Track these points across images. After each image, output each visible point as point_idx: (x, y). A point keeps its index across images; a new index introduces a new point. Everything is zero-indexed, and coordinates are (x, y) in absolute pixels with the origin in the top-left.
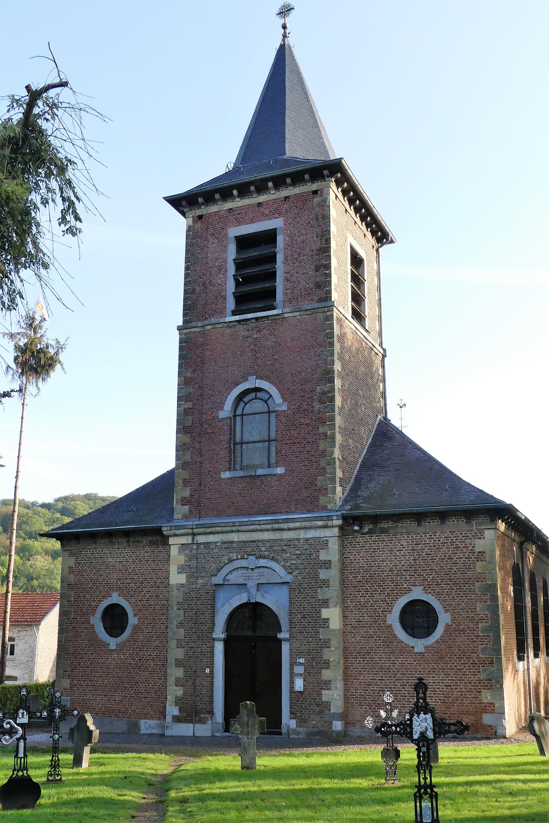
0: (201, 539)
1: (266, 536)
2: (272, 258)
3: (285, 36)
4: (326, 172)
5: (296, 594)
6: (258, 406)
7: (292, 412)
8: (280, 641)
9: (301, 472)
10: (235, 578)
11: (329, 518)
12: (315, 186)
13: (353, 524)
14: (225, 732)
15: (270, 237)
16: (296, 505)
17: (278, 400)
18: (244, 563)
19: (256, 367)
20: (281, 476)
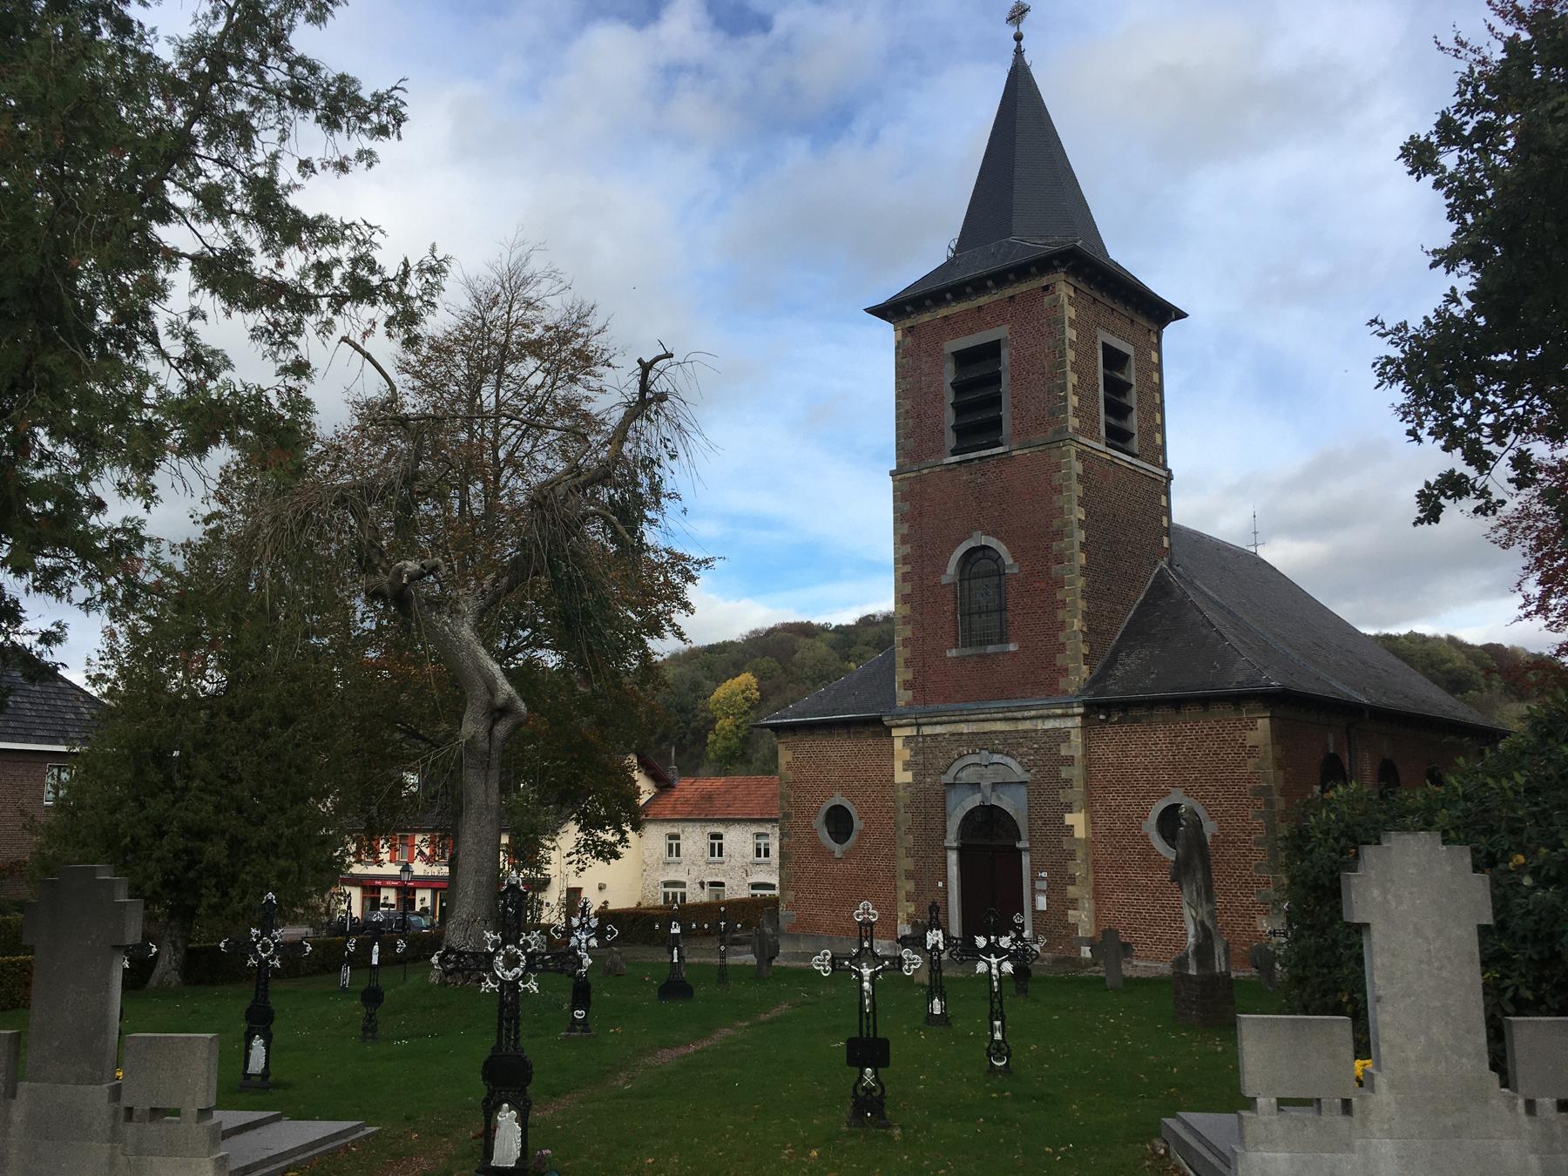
0: (927, 730)
1: (999, 726)
2: (996, 379)
3: (1019, 52)
4: (1056, 263)
8: (1019, 851)
10: (966, 776)
11: (1069, 705)
12: (1044, 281)
13: (1098, 713)
15: (993, 349)
18: (975, 759)
20: (1015, 654)
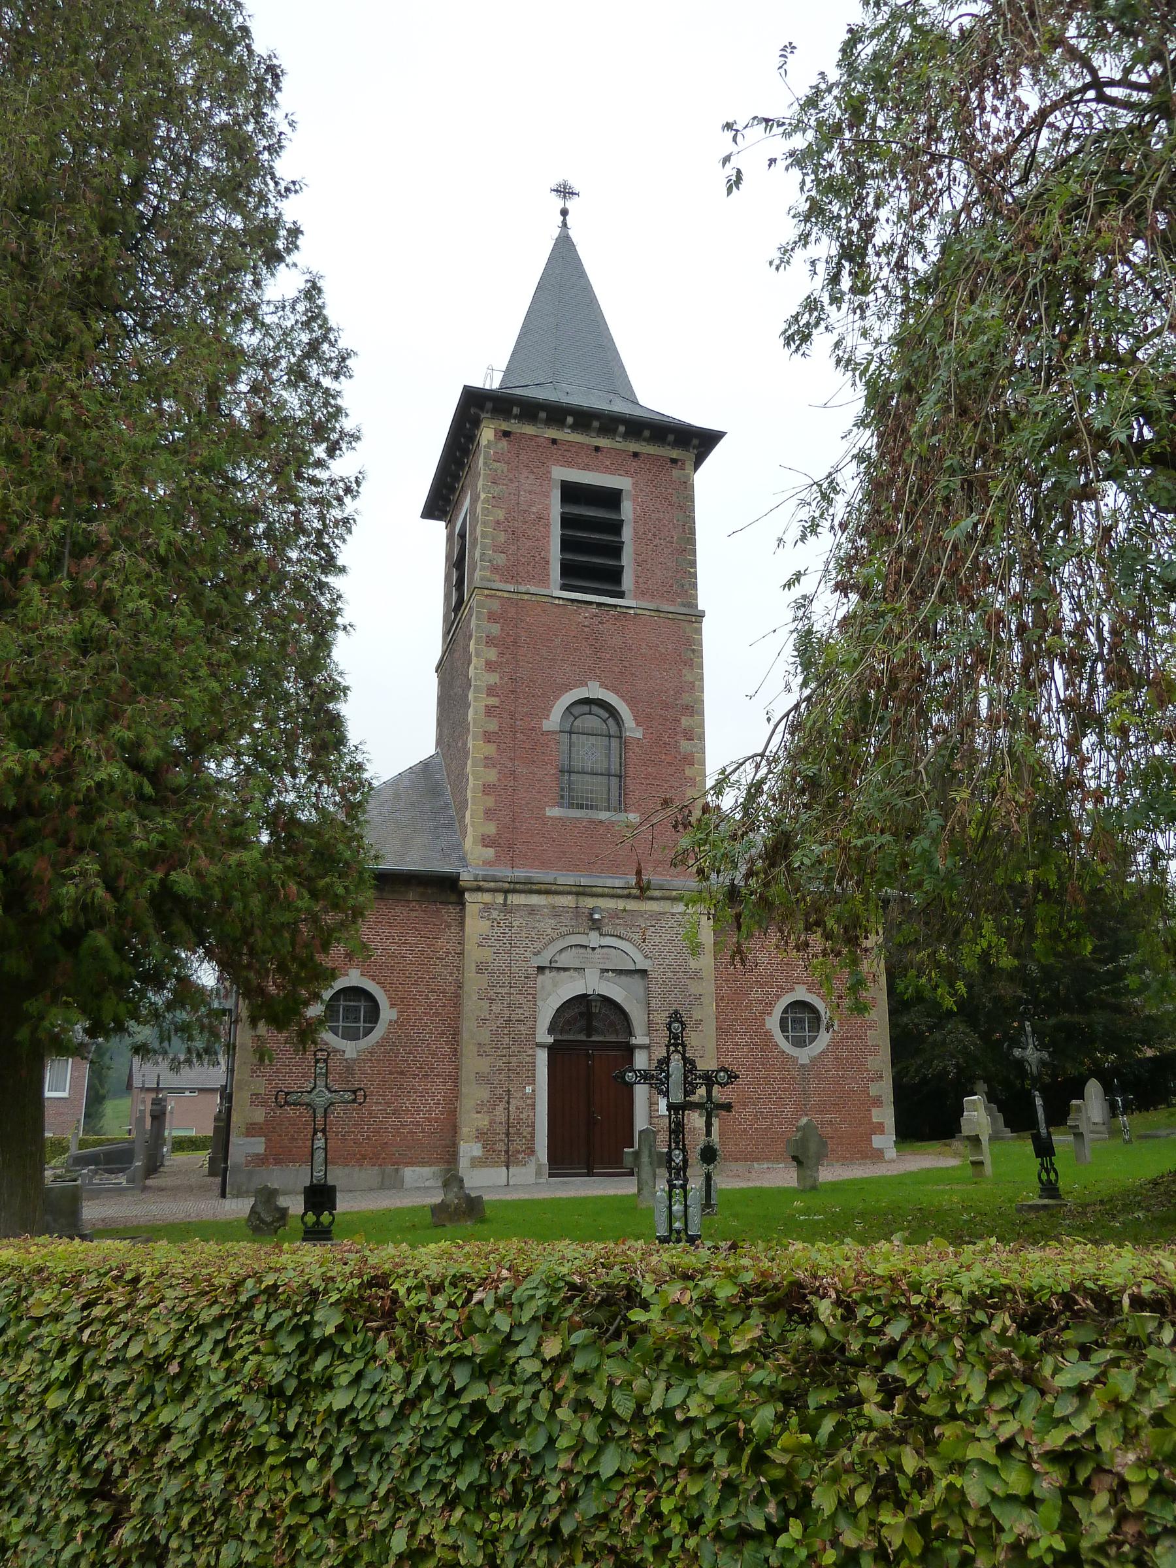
3: (564, 224)
12: (674, 454)
15: (611, 498)
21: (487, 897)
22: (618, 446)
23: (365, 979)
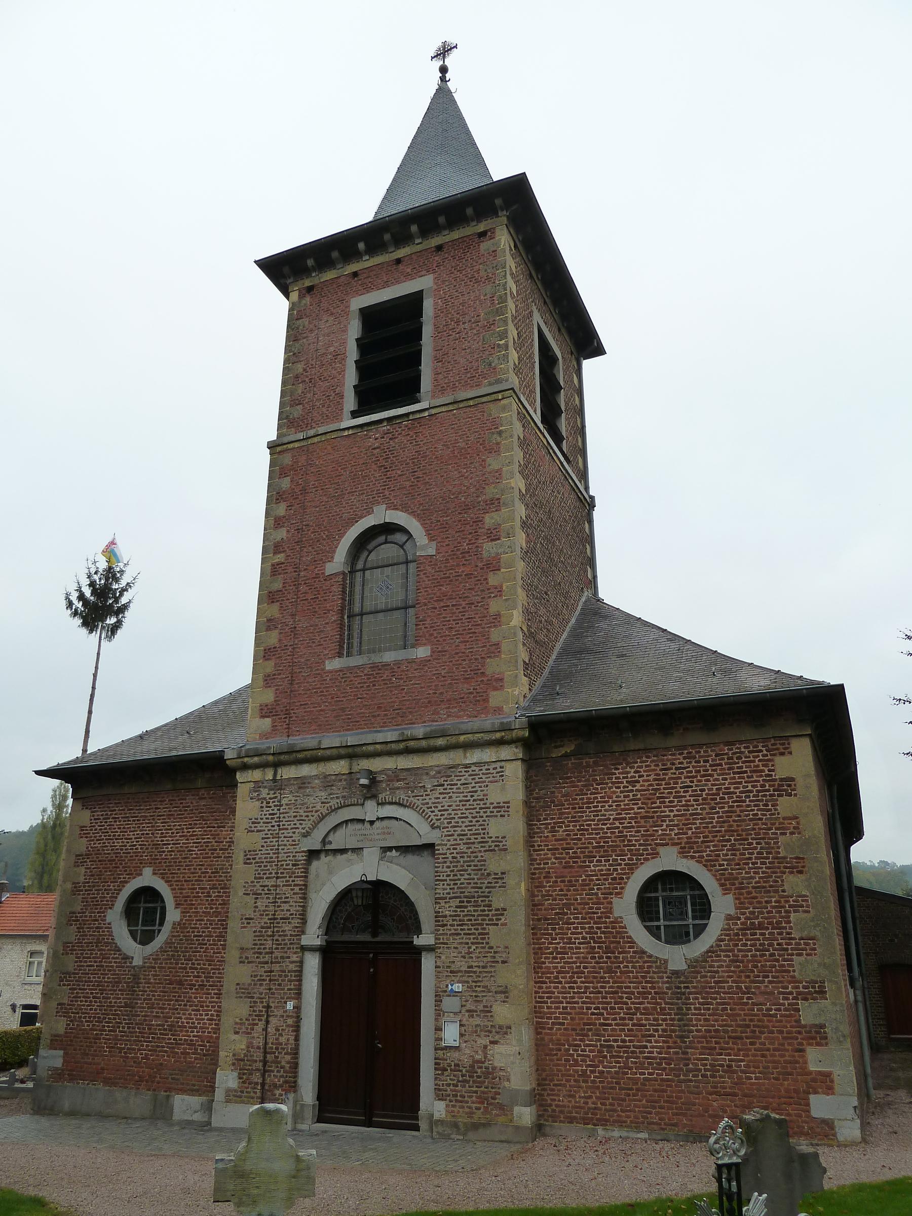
5: (448, 864)
6: (385, 551)
7: (444, 556)
8: (418, 951)
9: (457, 653)
12: (481, 227)
14: (319, 1121)
16: (449, 708)
17: (423, 542)
19: (387, 493)
20: (425, 662)
21: (257, 775)
22: (419, 248)
23: (155, 877)
